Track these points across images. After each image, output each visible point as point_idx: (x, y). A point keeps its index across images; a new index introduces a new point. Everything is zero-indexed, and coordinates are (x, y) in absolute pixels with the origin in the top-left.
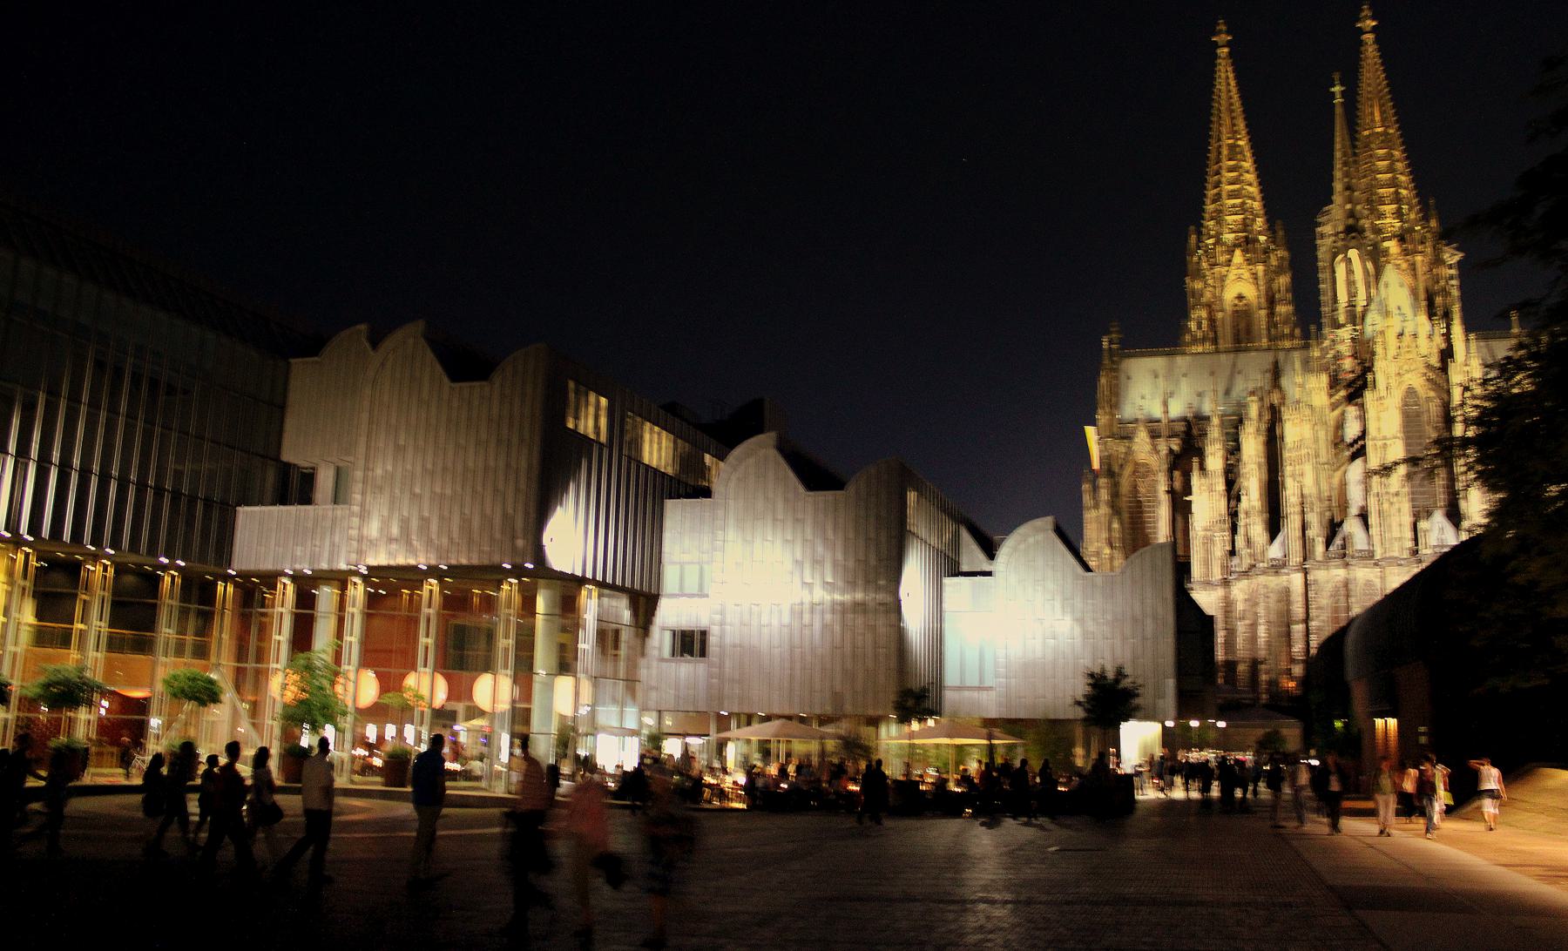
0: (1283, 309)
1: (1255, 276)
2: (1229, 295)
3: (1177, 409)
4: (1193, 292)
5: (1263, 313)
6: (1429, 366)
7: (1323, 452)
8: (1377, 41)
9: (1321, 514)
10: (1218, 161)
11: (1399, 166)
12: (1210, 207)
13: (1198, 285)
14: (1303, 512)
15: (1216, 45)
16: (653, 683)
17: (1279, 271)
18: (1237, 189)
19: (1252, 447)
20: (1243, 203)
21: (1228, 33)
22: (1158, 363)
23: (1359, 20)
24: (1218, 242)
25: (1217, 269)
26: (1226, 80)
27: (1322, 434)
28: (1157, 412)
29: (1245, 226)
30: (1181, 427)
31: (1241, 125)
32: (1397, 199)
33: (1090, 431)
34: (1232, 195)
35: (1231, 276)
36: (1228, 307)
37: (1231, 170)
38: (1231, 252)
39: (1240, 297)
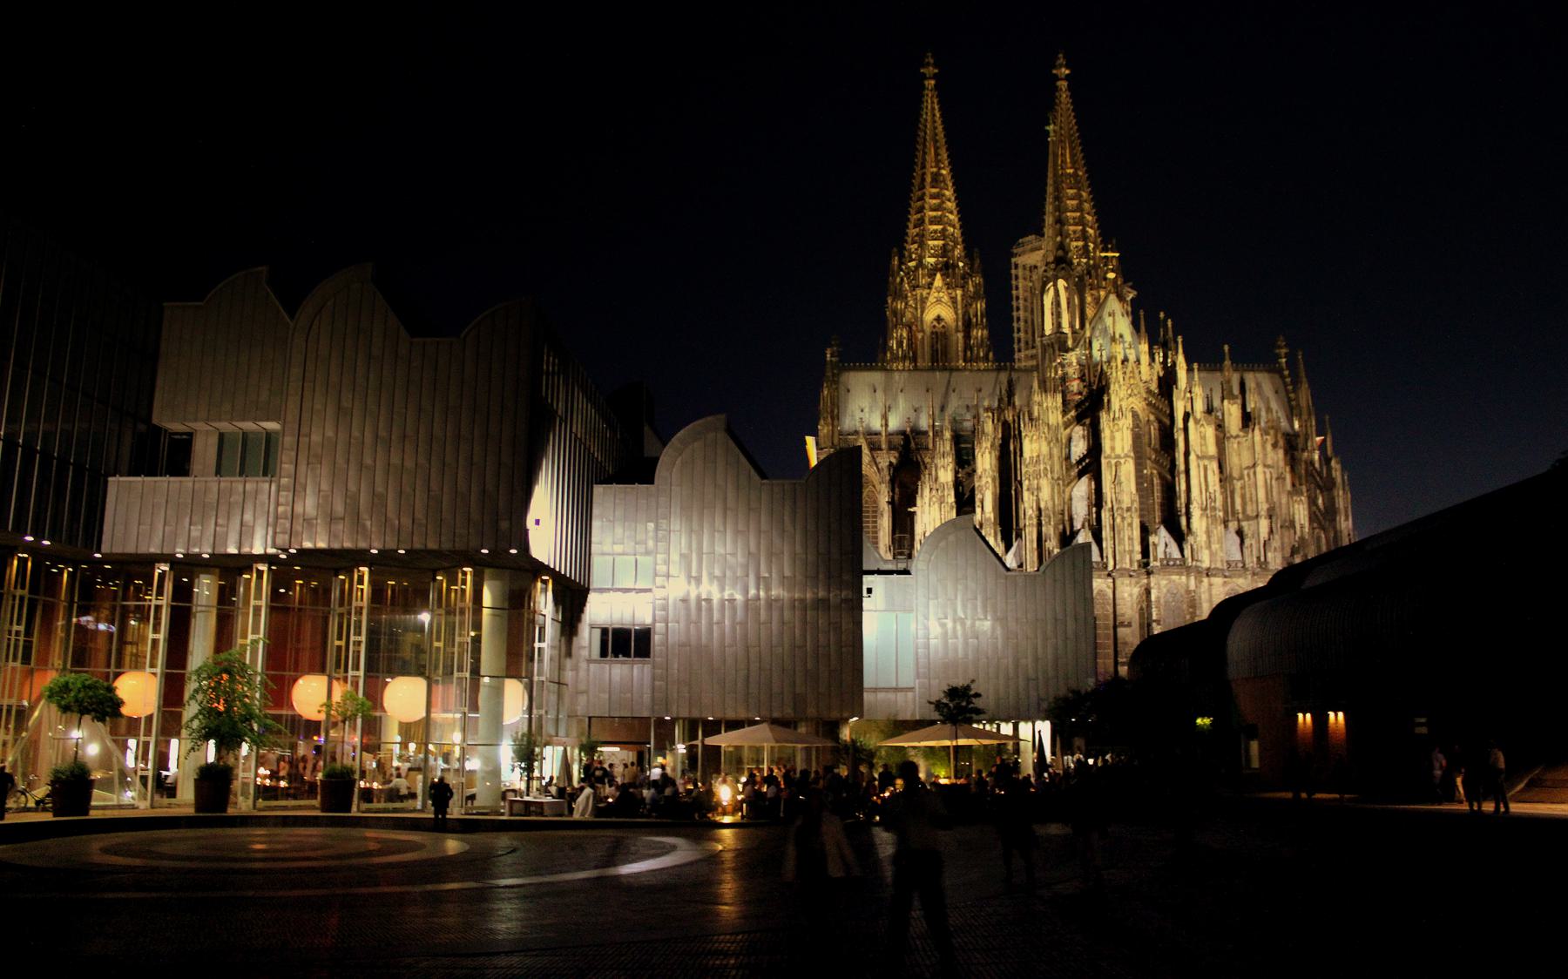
0: (978, 333)
1: (954, 300)
2: (929, 316)
3: (895, 423)
4: (895, 313)
5: (960, 335)
6: (1149, 391)
7: (1057, 467)
8: (1069, 88)
9: (1055, 527)
10: (922, 187)
11: (1086, 206)
12: (913, 231)
13: (900, 305)
14: (1040, 525)
15: (924, 77)
16: (582, 687)
17: (976, 297)
18: (939, 217)
19: (985, 462)
20: (944, 230)
21: (935, 66)
22: (876, 377)
23: (1055, 67)
24: (920, 264)
25: (918, 291)
26: (931, 110)
27: (1056, 451)
28: (876, 424)
29: (945, 251)
30: (899, 440)
31: (944, 155)
32: (1084, 237)
33: (810, 441)
34: (934, 221)
35: (932, 299)
36: (928, 330)
37: (933, 197)
38: (932, 276)
39: (939, 319)
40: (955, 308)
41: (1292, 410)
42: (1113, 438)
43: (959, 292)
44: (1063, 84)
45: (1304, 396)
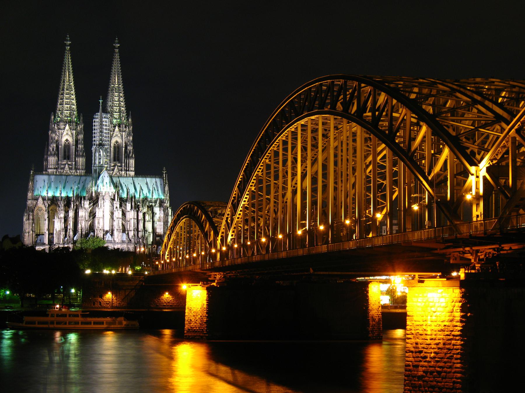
0: (80, 146)
1: (72, 134)
2: (64, 139)
5: (74, 147)
11: (122, 99)
12: (59, 106)
13: (53, 135)
18: (68, 102)
22: (46, 177)
23: (114, 43)
25: (60, 131)
27: (87, 214)
35: (65, 133)
36: (63, 144)
39: (67, 140)
41: (164, 192)
43: (74, 132)
45: (167, 188)
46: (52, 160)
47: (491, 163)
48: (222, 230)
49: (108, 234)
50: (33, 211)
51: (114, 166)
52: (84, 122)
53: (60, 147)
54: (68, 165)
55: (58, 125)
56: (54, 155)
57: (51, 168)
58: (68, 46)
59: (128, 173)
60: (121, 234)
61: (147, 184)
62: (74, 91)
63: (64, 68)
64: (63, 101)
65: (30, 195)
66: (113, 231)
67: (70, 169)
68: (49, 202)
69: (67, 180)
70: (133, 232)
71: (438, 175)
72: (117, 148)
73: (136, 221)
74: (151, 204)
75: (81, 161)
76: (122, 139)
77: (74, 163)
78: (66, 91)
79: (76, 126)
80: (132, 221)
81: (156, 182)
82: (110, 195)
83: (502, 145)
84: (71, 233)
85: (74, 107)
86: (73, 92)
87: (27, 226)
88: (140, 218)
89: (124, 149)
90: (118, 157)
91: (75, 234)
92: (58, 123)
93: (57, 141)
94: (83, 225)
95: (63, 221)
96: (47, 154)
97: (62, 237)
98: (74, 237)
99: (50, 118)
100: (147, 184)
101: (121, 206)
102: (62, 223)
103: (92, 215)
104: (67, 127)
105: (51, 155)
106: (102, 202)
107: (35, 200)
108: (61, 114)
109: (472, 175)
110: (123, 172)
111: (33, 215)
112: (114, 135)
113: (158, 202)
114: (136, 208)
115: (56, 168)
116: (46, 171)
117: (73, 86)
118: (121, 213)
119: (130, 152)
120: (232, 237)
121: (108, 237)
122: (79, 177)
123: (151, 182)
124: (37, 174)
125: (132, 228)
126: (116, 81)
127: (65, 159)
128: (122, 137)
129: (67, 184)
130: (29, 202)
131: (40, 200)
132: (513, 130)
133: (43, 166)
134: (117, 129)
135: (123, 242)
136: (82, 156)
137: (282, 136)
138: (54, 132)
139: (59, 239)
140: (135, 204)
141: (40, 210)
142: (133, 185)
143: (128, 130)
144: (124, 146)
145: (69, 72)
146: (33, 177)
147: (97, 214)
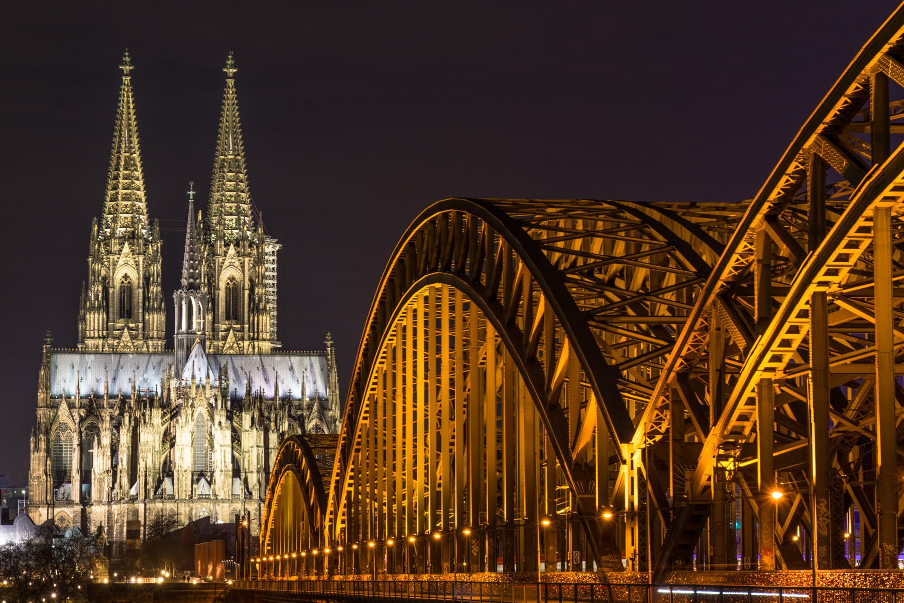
3: (84, 391)
5: (141, 291)
8: (236, 85)
10: (117, 169)
11: (242, 185)
12: (109, 204)
13: (97, 267)
22: (76, 358)
23: (225, 66)
24: (113, 234)
25: (111, 257)
27: (157, 438)
28: (73, 391)
29: (134, 223)
35: (121, 262)
36: (117, 284)
39: (126, 277)
40: (138, 269)
42: (181, 436)
43: (141, 258)
44: (231, 82)
45: (334, 377)
46: (94, 320)
47: (650, 441)
48: (330, 508)
49: (203, 481)
50: (47, 433)
51: (228, 330)
52: (162, 236)
53: (111, 290)
54: (129, 329)
55: (107, 245)
56: (99, 308)
57: (93, 338)
58: (127, 75)
59: (256, 344)
60: (230, 480)
61: (291, 368)
62: (140, 170)
63: (118, 122)
64: (118, 193)
65: (41, 396)
66: (212, 473)
67: (133, 337)
68: (83, 412)
69: (122, 363)
70: (255, 475)
71: (585, 449)
72: (234, 291)
73: (262, 450)
74: (299, 412)
75: (156, 320)
76: (243, 271)
77: (141, 325)
78: (122, 172)
79: (145, 245)
80: (255, 449)
81: (311, 366)
82: (208, 396)
83: (659, 404)
84: (125, 481)
85: (142, 205)
86: (138, 174)
87: (38, 464)
88: (271, 446)
89: (247, 292)
90: (236, 310)
91: (133, 480)
92: (107, 240)
93: (105, 279)
94: (149, 460)
95: (109, 453)
96: (85, 307)
97: (106, 489)
98: (131, 487)
99: (91, 229)
100: (291, 368)
101: (229, 418)
102: (106, 458)
103: (169, 439)
104: (126, 249)
105: (92, 308)
106: (189, 411)
107: (52, 407)
108: (114, 220)
109: (624, 462)
110: (246, 343)
111: (48, 443)
112: (227, 263)
113: (315, 407)
114: (262, 422)
115: (104, 337)
116: (83, 342)
117: (138, 159)
118: (228, 433)
119: (260, 300)
120: (343, 526)
121: (202, 487)
122: (147, 357)
123: (301, 363)
124: (58, 353)
125: (254, 468)
126: (230, 147)
127: (121, 317)
128: (243, 267)
129: (121, 371)
130: (40, 412)
131: (64, 406)
132: (673, 374)
133: (77, 332)
134: (232, 250)
135: (233, 498)
136: (159, 309)
137: (398, 317)
138: (99, 260)
139: (100, 491)
140: (261, 414)
141: (64, 427)
142: (261, 371)
143: (255, 252)
144: (246, 287)
145: (130, 131)
146: (48, 357)
147: (178, 441)
